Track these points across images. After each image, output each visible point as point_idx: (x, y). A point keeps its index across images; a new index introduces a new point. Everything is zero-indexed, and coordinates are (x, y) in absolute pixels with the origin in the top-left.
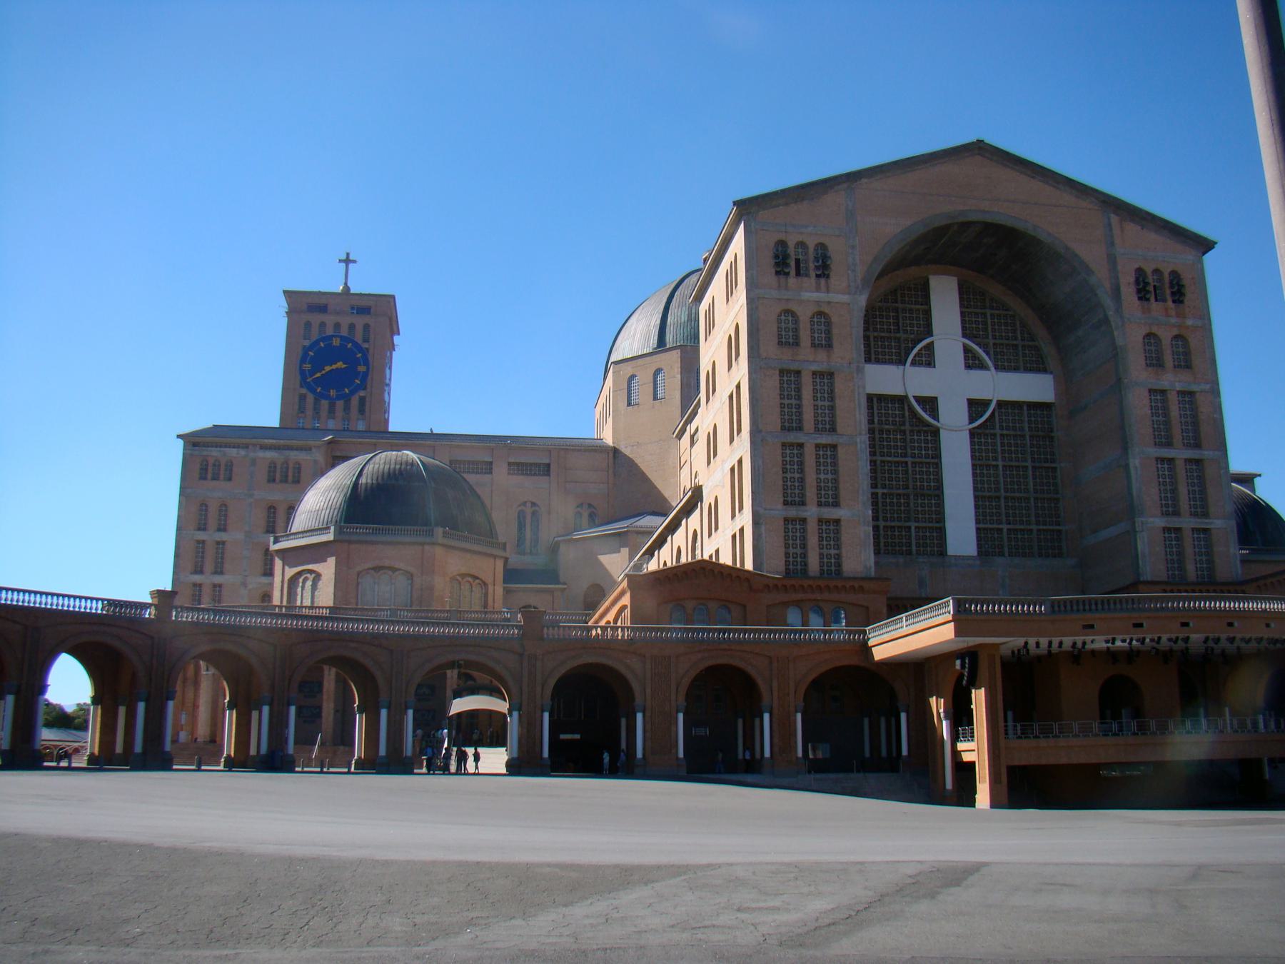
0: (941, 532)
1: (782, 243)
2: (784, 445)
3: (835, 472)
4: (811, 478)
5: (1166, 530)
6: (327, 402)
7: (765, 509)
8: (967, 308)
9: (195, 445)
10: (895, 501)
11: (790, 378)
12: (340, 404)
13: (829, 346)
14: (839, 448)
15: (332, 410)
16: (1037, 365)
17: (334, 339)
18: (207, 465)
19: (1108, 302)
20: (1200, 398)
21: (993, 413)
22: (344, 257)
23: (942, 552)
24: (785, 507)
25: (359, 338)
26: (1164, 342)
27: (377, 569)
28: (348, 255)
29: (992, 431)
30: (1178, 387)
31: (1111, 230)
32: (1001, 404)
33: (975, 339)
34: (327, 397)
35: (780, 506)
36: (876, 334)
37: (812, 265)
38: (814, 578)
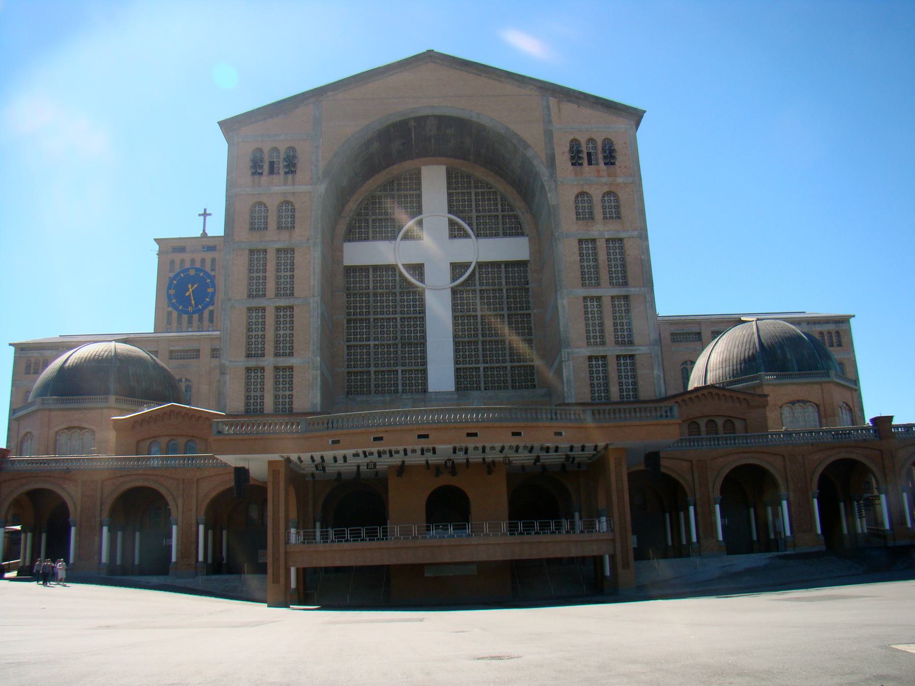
0: (424, 372)
2: (250, 309)
3: (292, 328)
4: (270, 335)
5: (590, 358)
6: (187, 316)
7: (230, 361)
8: (456, 189)
9: (22, 349)
10: (386, 350)
15: (190, 322)
16: (514, 230)
17: (191, 270)
18: (30, 363)
19: (543, 170)
20: (628, 244)
21: (473, 272)
22: (202, 212)
23: (425, 391)
24: (247, 359)
25: (208, 268)
26: (594, 199)
28: (205, 210)
29: (473, 288)
31: (549, 110)
32: (480, 265)
33: (460, 214)
34: (187, 312)
35: (243, 359)
36: (374, 217)
37: (281, 165)
38: (269, 415)
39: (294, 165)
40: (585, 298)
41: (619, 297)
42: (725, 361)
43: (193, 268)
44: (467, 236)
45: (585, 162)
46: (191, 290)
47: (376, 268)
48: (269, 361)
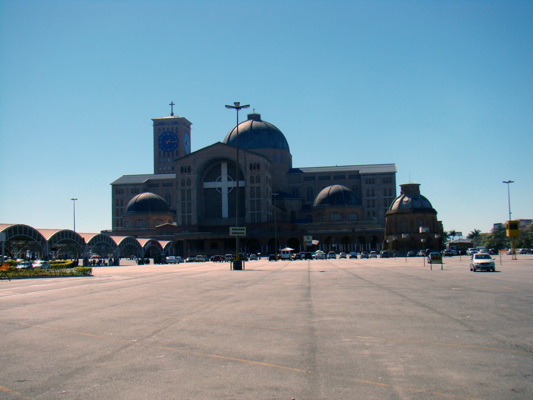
2: (182, 203)
5: (251, 213)
11: (183, 191)
12: (171, 153)
13: (190, 185)
14: (191, 203)
15: (169, 156)
23: (222, 217)
25: (175, 132)
27: (139, 220)
28: (172, 102)
30: (257, 186)
39: (190, 170)
40: (251, 201)
41: (259, 200)
42: (319, 199)
43: (168, 132)
45: (253, 168)
46: (168, 142)
47: (211, 188)
48: (186, 214)
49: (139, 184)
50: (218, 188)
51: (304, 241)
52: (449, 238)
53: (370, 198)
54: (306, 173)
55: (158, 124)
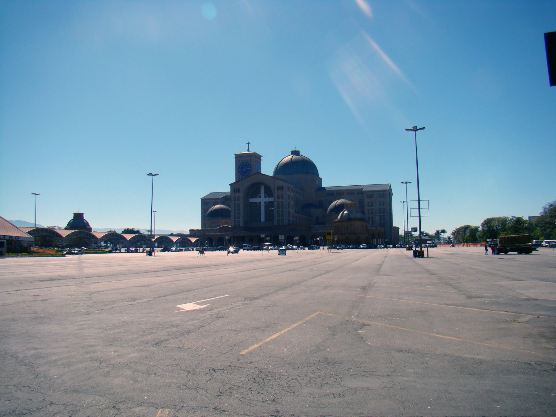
1: (234, 189)
5: (278, 219)
13: (239, 200)
21: (268, 204)
25: (249, 162)
30: (281, 201)
32: (269, 202)
40: (278, 211)
44: (267, 197)
48: (237, 220)
49: (218, 199)
50: (258, 202)
51: (279, 238)
52: (441, 235)
53: (370, 207)
54: (328, 191)
55: (239, 157)
